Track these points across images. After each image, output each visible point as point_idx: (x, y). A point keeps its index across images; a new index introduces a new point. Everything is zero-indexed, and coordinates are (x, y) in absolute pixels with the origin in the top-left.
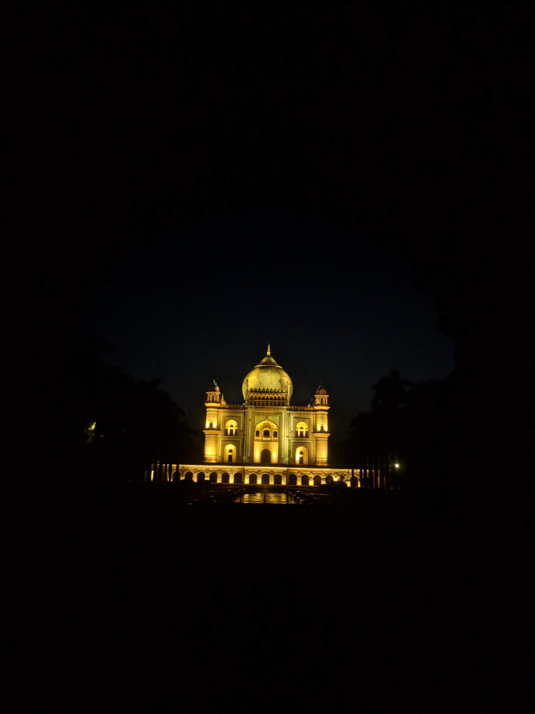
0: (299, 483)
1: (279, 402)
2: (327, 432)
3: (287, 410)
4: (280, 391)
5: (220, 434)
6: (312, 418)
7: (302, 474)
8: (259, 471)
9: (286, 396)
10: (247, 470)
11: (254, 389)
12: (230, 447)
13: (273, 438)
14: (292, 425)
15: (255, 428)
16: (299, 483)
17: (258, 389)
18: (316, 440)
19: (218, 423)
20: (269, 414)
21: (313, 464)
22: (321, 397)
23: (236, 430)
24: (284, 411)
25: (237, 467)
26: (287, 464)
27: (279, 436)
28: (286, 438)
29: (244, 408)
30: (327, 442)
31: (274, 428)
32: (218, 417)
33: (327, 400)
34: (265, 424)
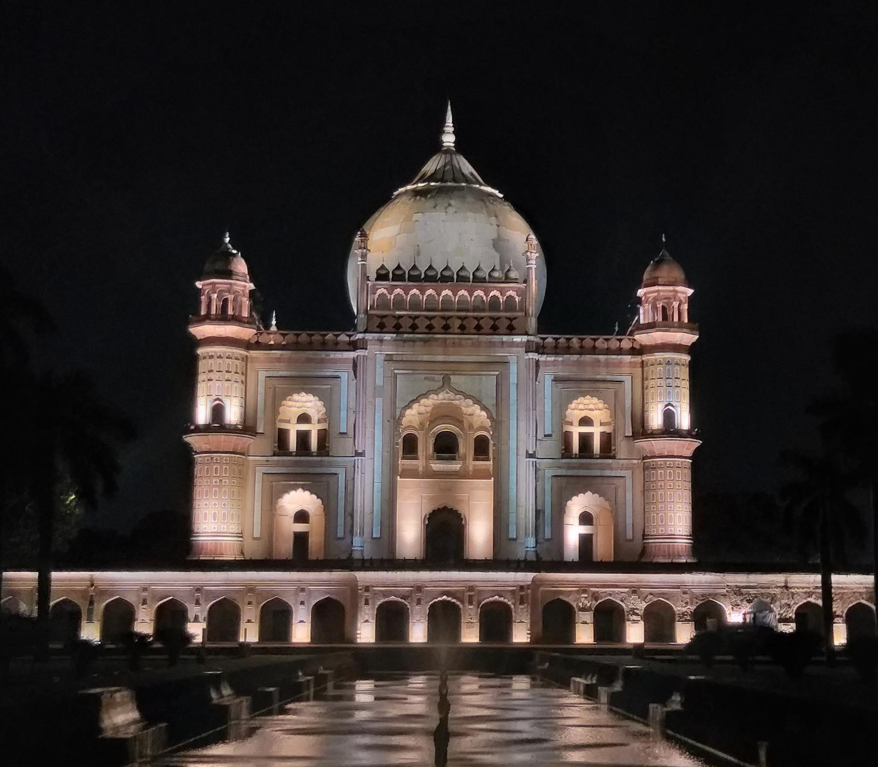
0: (584, 635)
1: (497, 322)
2: (688, 434)
3: (529, 348)
4: (496, 274)
5: (258, 448)
6: (627, 379)
7: (595, 597)
8: (419, 588)
9: (523, 293)
10: (367, 589)
11: (391, 267)
12: (298, 499)
13: (473, 464)
14: (548, 409)
15: (396, 421)
16: (584, 635)
17: (406, 267)
18: (645, 468)
19: (245, 407)
20: (457, 368)
21: (636, 557)
22: (665, 295)
23: (323, 436)
24: (515, 352)
25: (324, 575)
26: (532, 557)
27: (498, 452)
28: (525, 462)
29: (354, 346)
30: (688, 473)
31: (477, 423)
32: (245, 383)
33: (685, 307)
34: (436, 407)
